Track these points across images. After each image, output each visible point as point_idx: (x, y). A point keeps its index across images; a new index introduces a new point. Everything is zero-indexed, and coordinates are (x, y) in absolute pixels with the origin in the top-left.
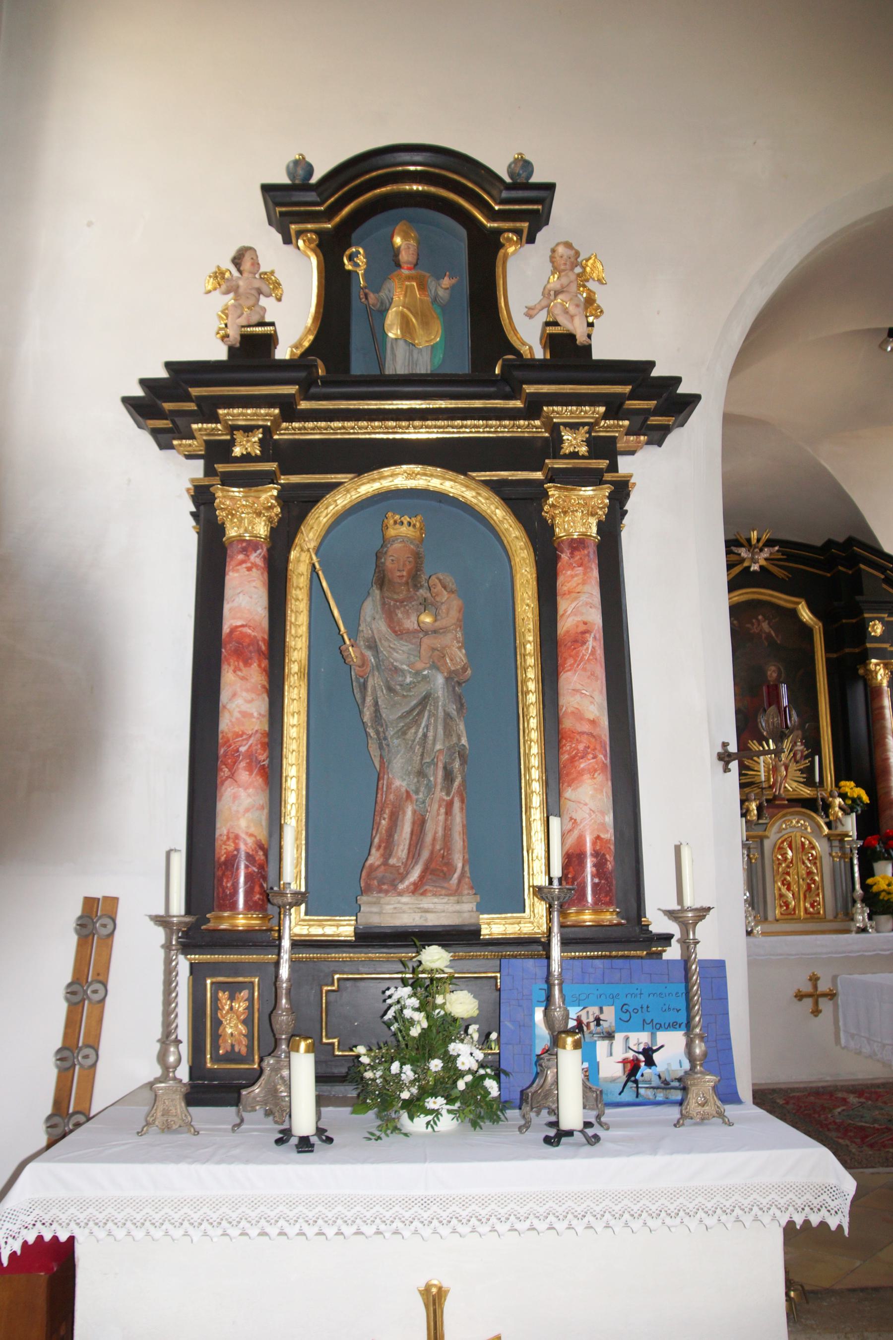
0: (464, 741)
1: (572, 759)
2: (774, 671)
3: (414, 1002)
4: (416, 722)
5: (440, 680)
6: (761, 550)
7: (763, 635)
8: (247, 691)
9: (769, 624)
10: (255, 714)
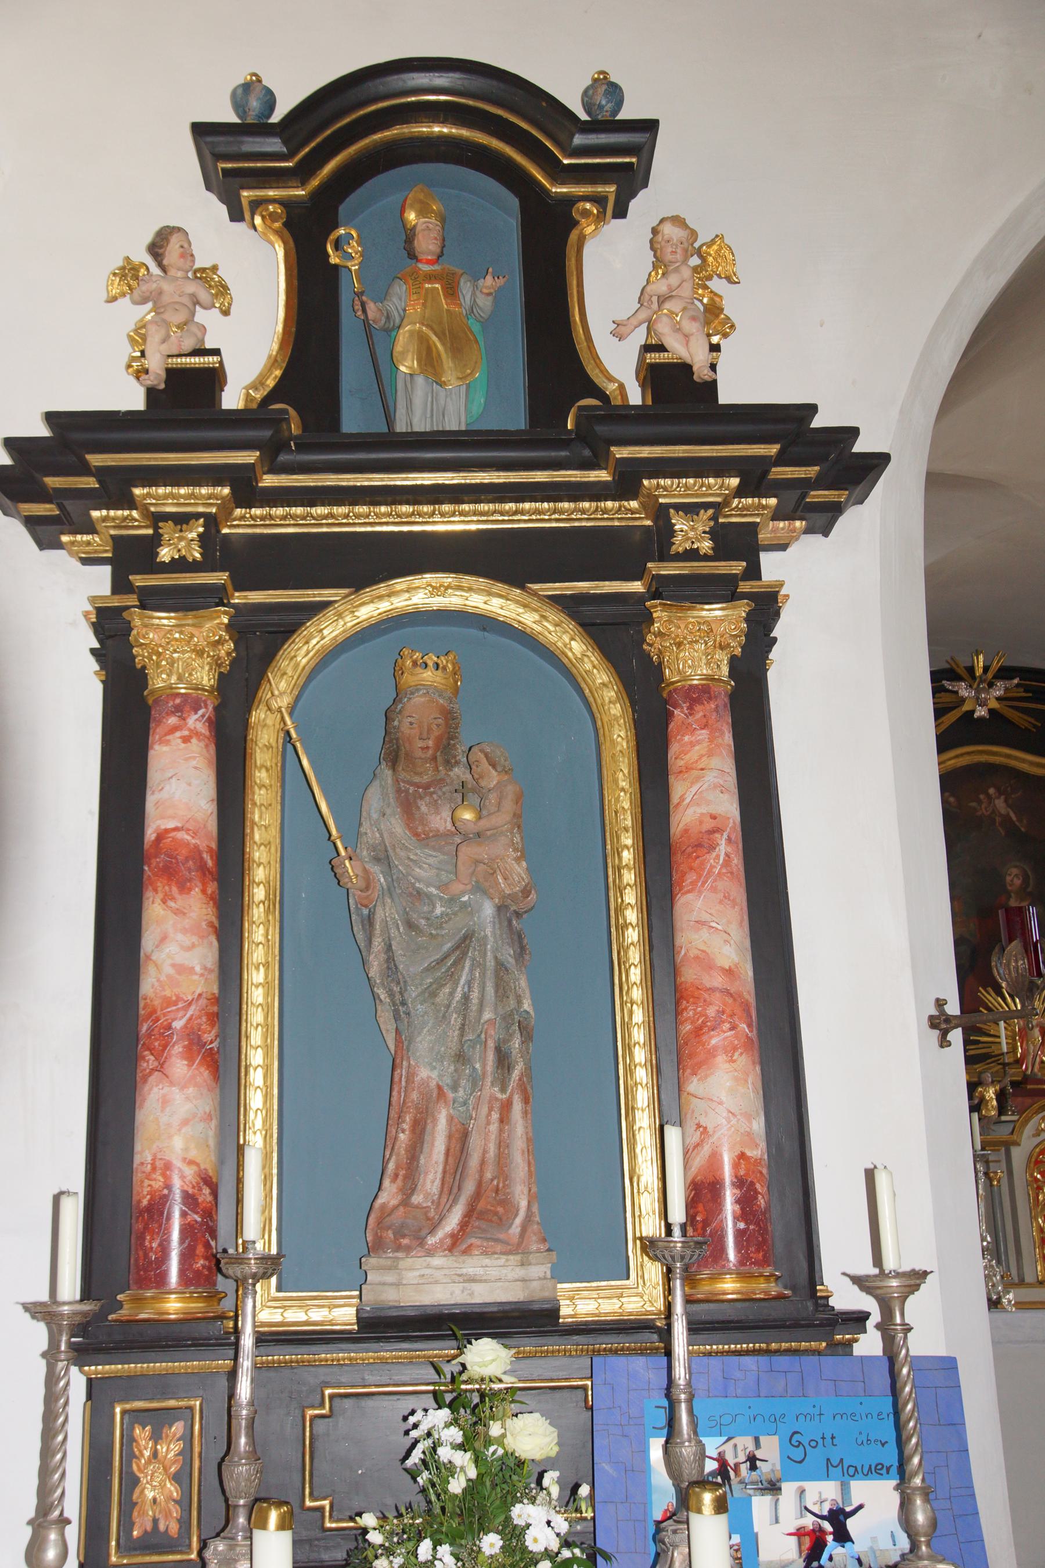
0: (527, 1005)
1: (698, 1032)
2: (1016, 875)
3: (455, 1434)
4: (452, 976)
5: (488, 910)
6: (991, 685)
8: (184, 931)
9: (1006, 801)
10: (198, 969)
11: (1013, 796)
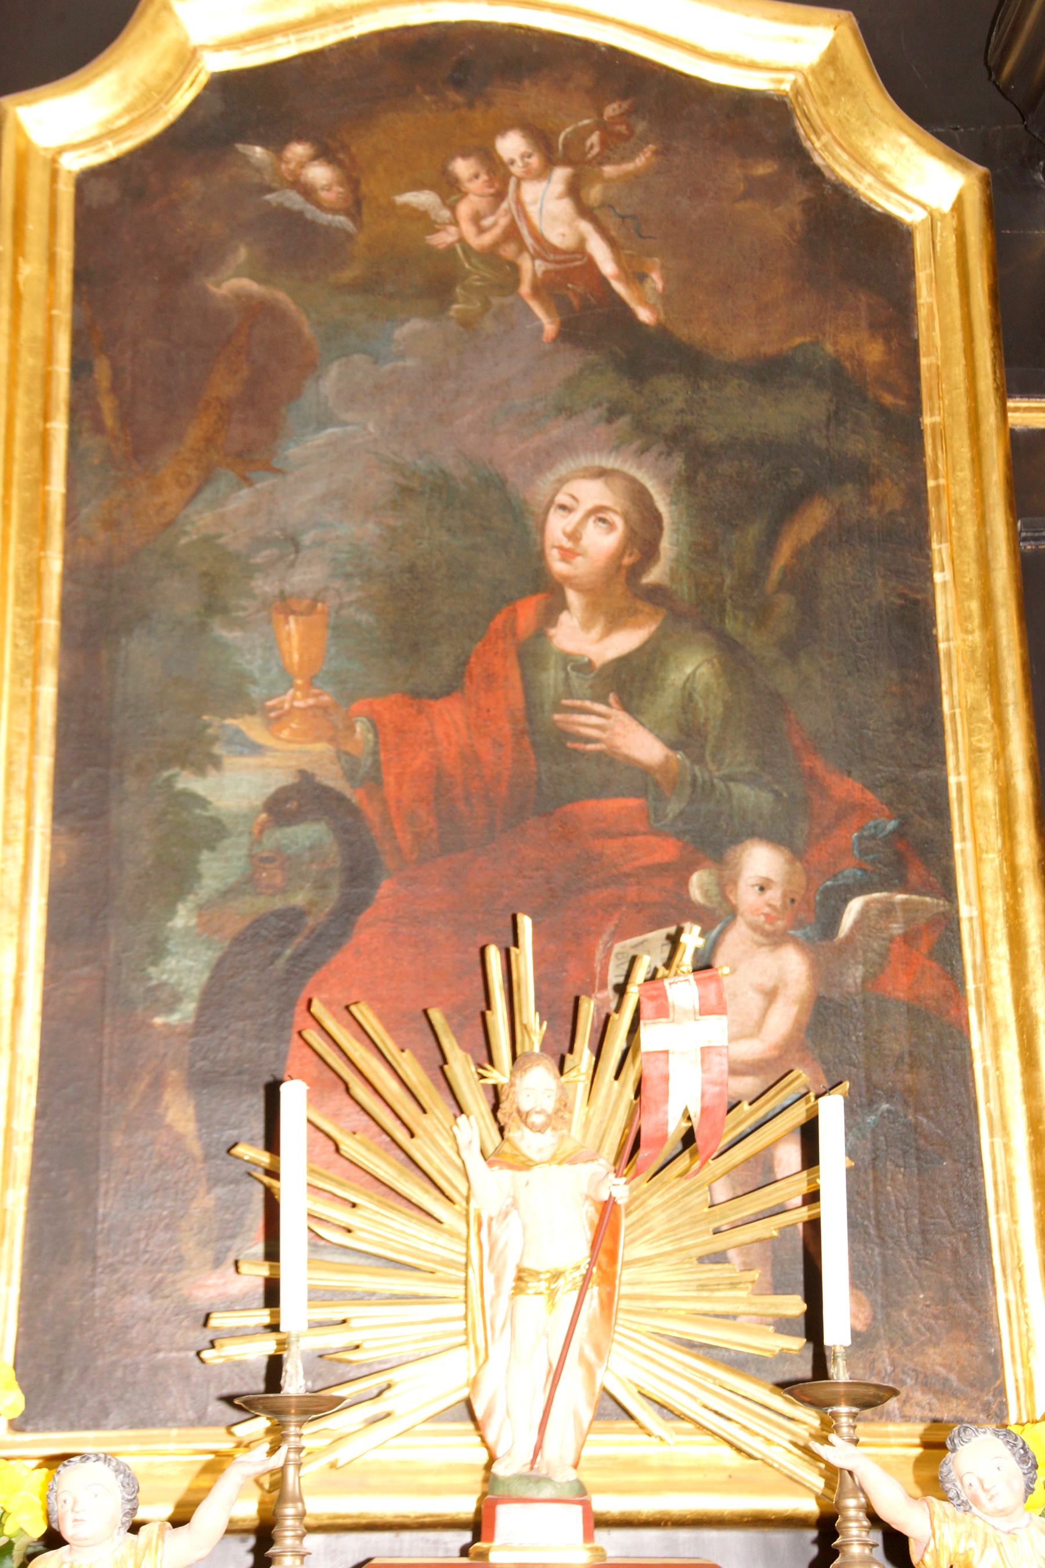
2: (598, 513)
7: (530, 268)
9: (574, 190)
11: (609, 170)
